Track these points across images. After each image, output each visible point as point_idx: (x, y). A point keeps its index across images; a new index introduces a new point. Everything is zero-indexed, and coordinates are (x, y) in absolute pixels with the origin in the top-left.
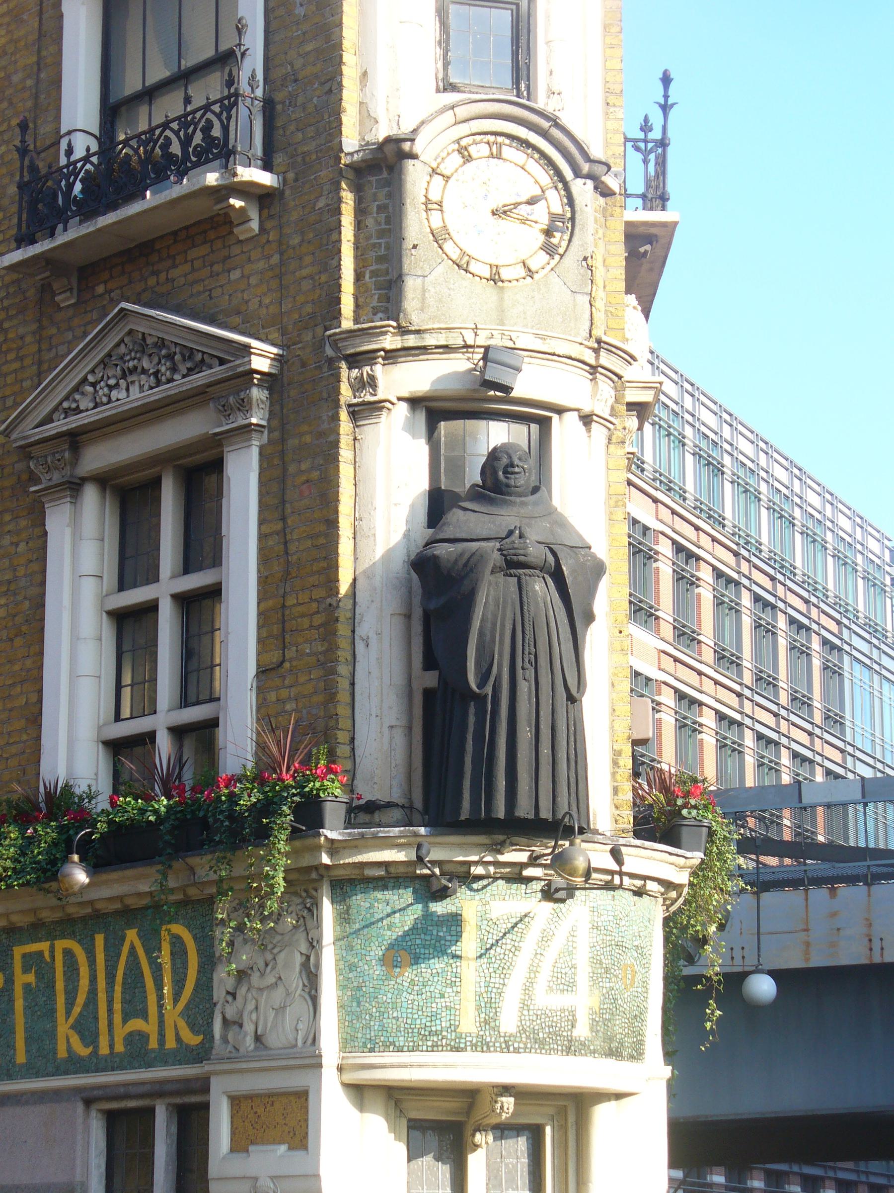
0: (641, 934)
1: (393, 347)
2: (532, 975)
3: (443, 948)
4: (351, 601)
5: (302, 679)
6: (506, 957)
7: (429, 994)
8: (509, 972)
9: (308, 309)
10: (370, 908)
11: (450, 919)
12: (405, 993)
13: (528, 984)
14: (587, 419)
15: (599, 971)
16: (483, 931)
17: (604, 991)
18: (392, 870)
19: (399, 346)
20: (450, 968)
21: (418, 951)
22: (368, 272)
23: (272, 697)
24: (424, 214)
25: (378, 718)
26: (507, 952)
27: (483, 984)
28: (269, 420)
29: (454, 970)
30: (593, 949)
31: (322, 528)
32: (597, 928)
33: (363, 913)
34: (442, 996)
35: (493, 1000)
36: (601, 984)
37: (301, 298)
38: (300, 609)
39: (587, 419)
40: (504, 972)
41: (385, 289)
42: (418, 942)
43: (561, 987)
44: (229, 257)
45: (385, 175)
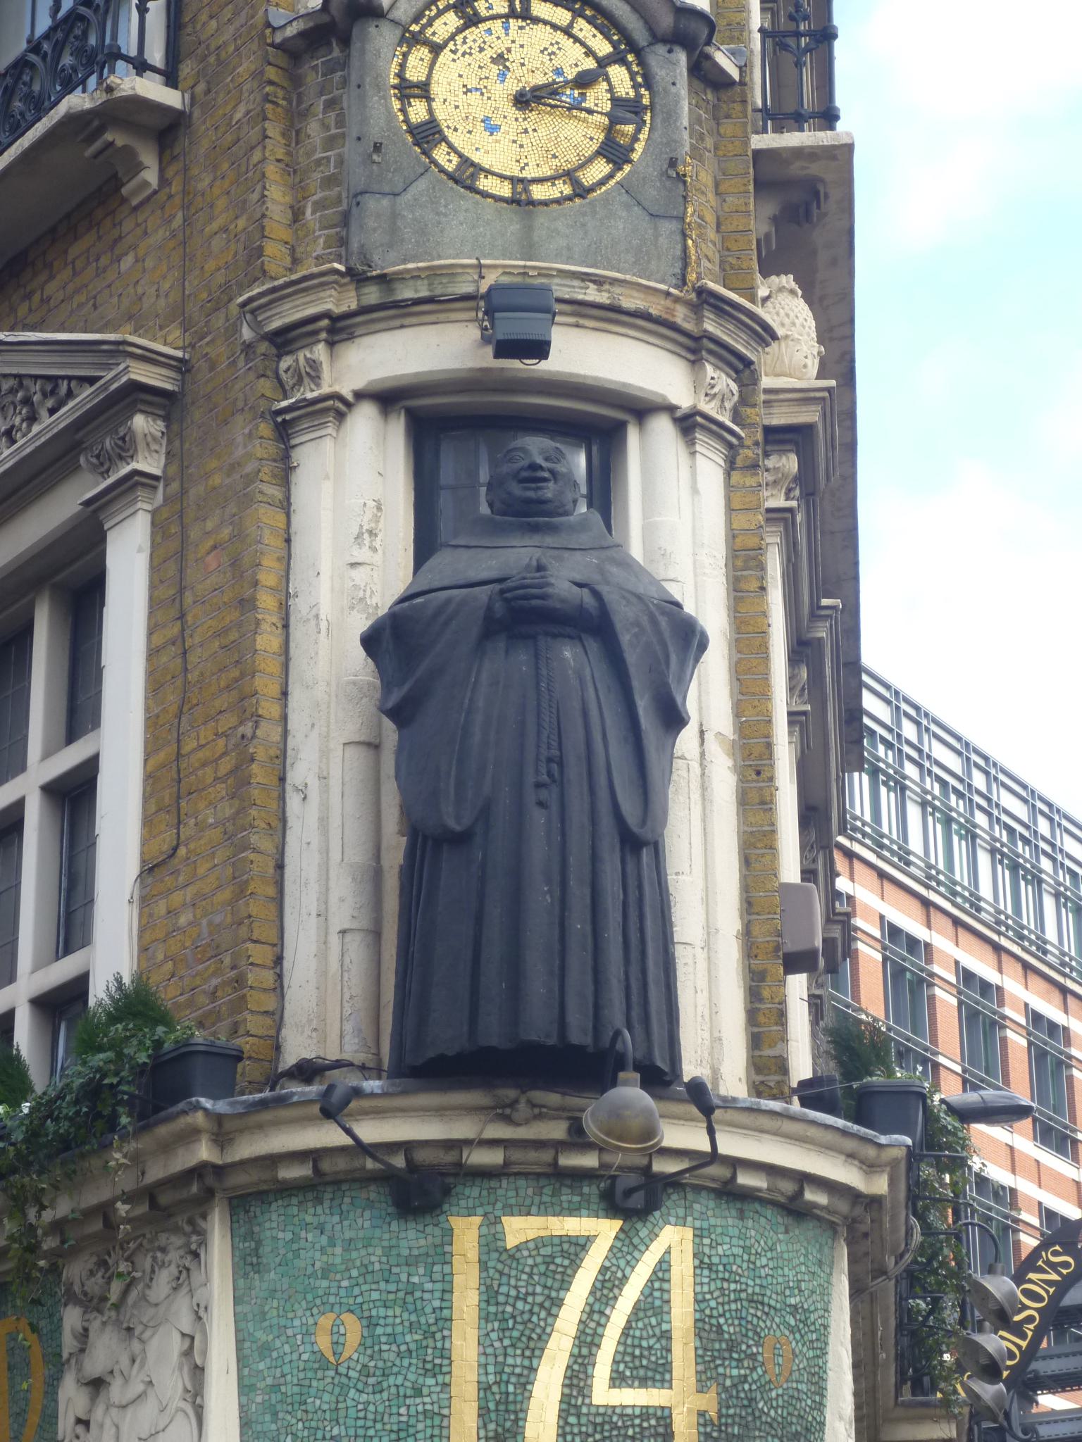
0: (803, 1285)
1: (343, 308)
2: (585, 1351)
3: (419, 1303)
4: (280, 729)
5: (201, 871)
6: (535, 1319)
7: (393, 1390)
8: (540, 1345)
9: (220, 278)
10: (292, 1241)
11: (431, 1252)
12: (352, 1392)
13: (576, 1367)
14: (688, 424)
15: (717, 1346)
16: (491, 1272)
17: (728, 1383)
18: (326, 1166)
19: (354, 306)
20: (431, 1344)
21: (374, 1313)
22: (309, 205)
23: (161, 908)
24: (396, 105)
25: (322, 919)
26: (536, 1309)
27: (491, 1369)
28: (164, 471)
29: (439, 1345)
30: (703, 1305)
31: (233, 615)
32: (710, 1267)
33: (282, 1252)
34: (418, 1392)
35: (511, 1398)
36: (721, 1370)
37: (211, 265)
38: (201, 755)
39: (688, 424)
40: (532, 1344)
41: (335, 226)
42: (375, 1295)
43: (642, 1372)
44: (120, 238)
45: (336, 52)
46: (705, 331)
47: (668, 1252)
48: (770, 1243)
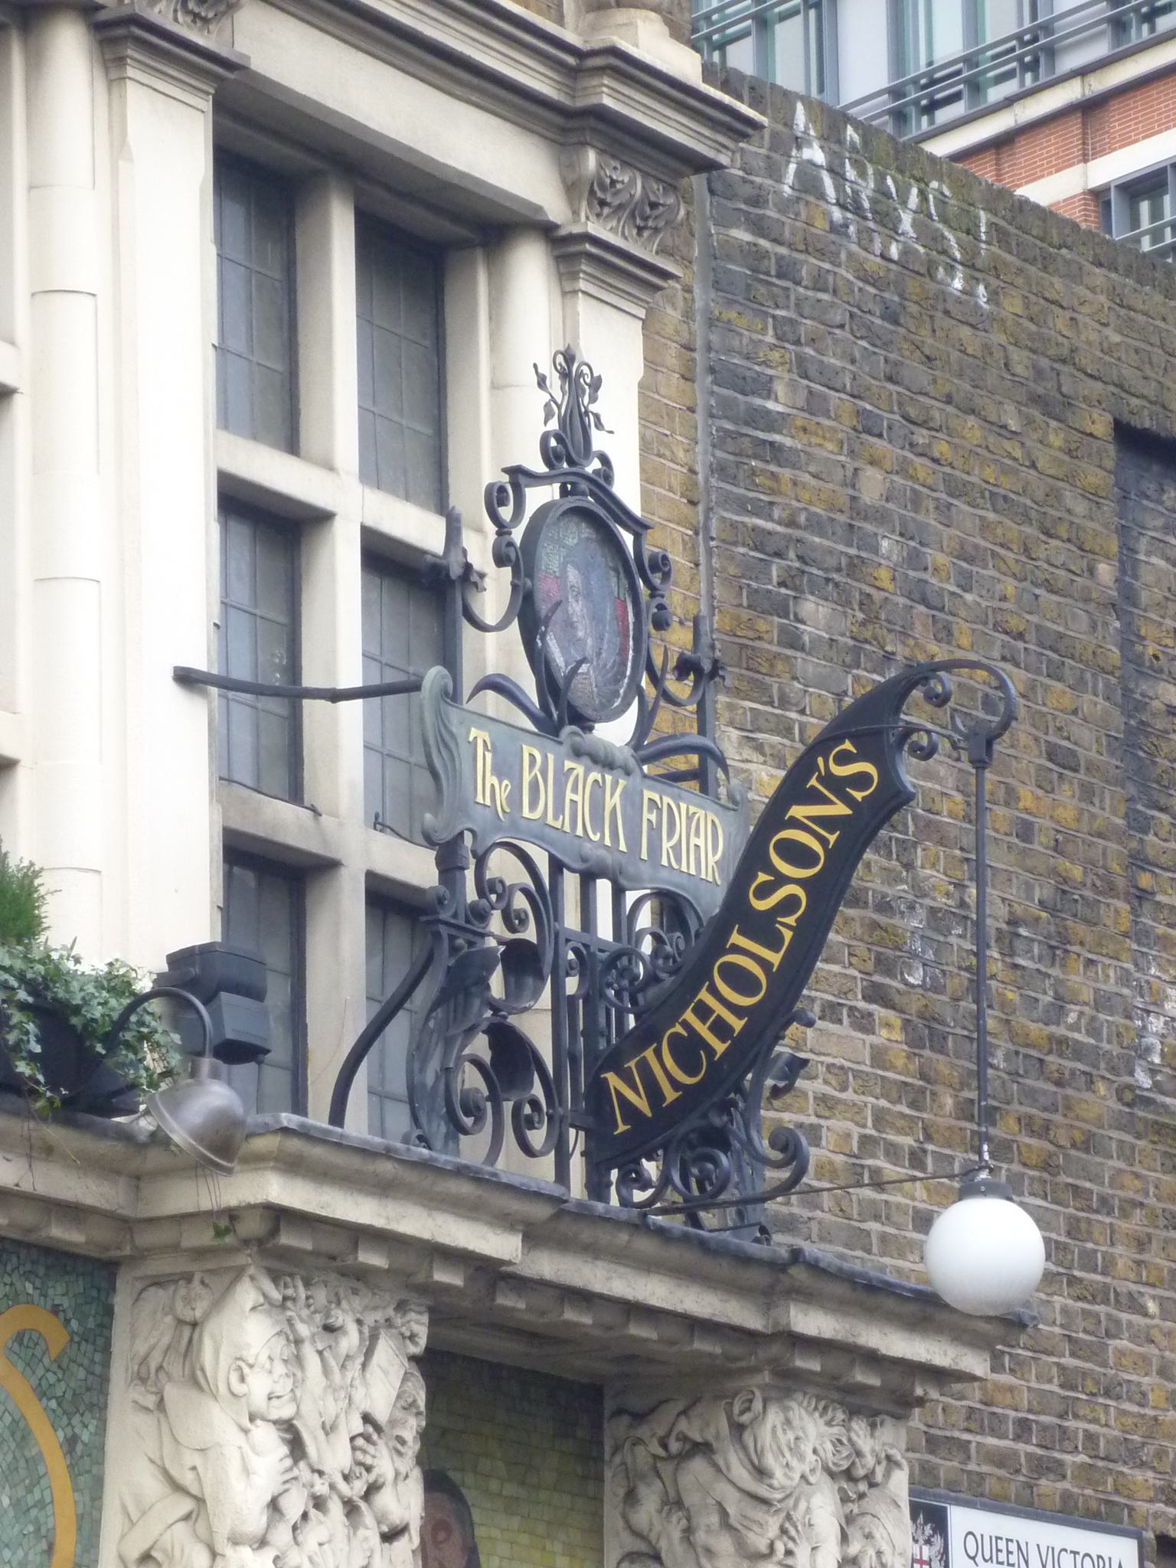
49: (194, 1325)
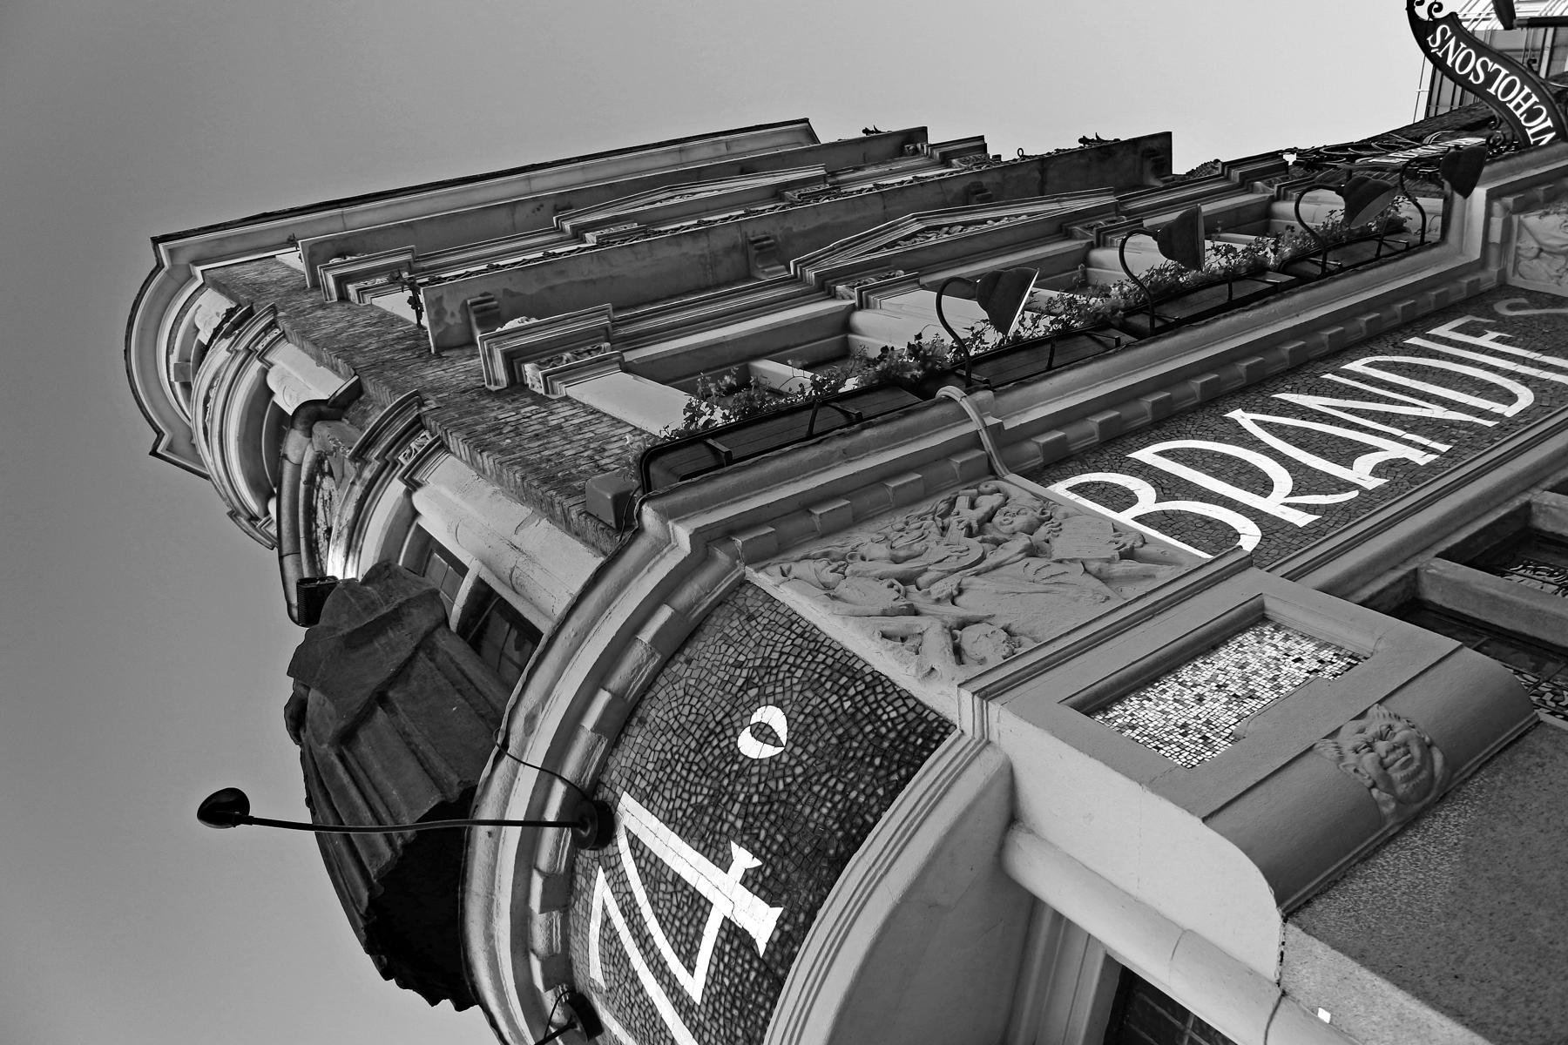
32: (655, 789)
46: (377, 458)
47: (628, 832)
48: (681, 693)
49: (1541, 250)
